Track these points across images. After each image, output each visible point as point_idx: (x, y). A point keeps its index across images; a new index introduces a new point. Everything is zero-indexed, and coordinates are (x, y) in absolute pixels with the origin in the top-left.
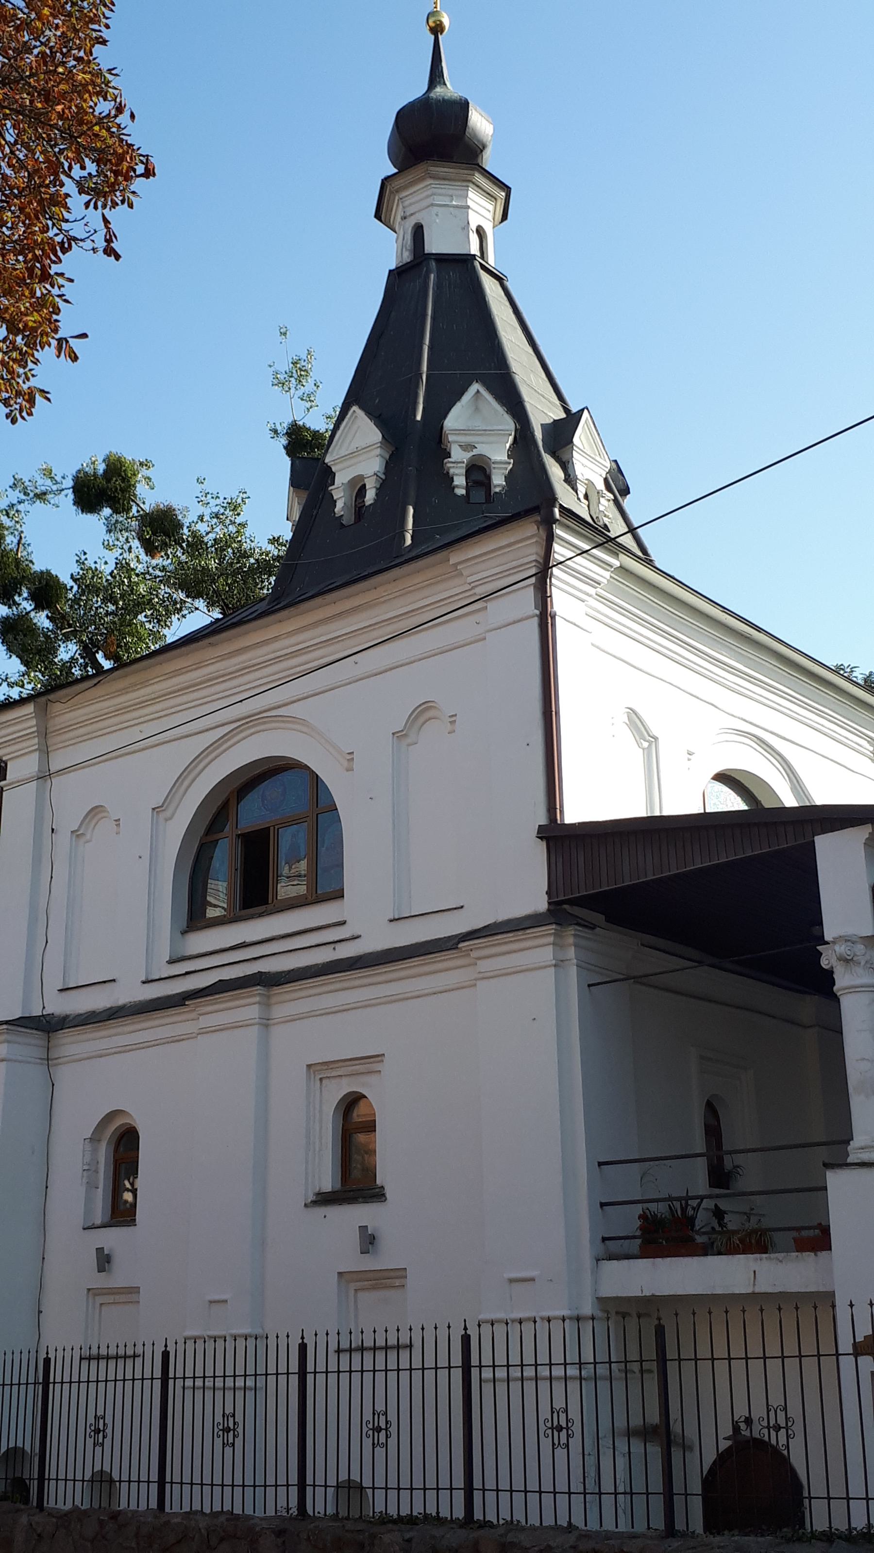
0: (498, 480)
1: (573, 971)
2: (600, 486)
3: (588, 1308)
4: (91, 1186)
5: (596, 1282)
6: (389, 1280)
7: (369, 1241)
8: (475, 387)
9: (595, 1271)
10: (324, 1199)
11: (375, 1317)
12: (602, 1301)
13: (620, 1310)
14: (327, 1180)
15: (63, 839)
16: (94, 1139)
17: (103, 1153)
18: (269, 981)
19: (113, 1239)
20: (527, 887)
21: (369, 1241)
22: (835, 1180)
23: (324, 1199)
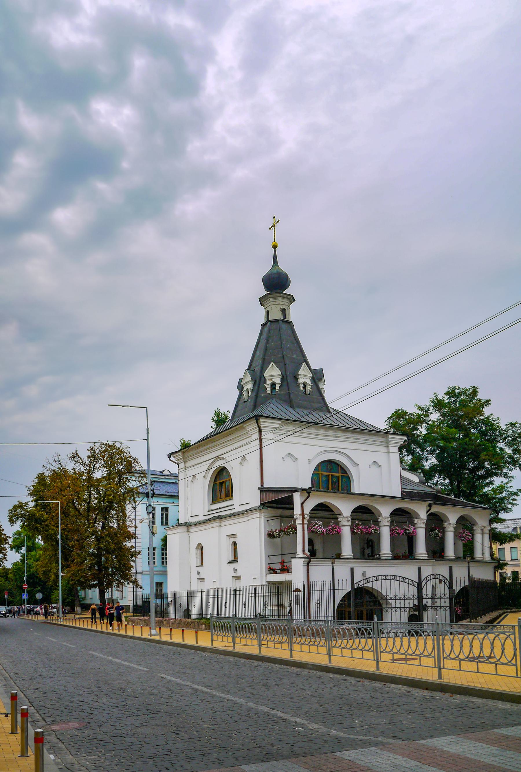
0: (278, 388)
1: (263, 518)
2: (309, 382)
3: (264, 584)
4: (197, 558)
5: (266, 579)
6: (238, 578)
7: (235, 570)
8: (272, 363)
9: (266, 576)
10: (231, 562)
11: (239, 585)
12: (269, 583)
13: (272, 584)
14: (231, 558)
15: (189, 482)
16: (197, 548)
17: (199, 551)
18: (219, 518)
19: (200, 569)
20: (256, 500)
21: (235, 570)
22: (293, 560)
23: (231, 562)
